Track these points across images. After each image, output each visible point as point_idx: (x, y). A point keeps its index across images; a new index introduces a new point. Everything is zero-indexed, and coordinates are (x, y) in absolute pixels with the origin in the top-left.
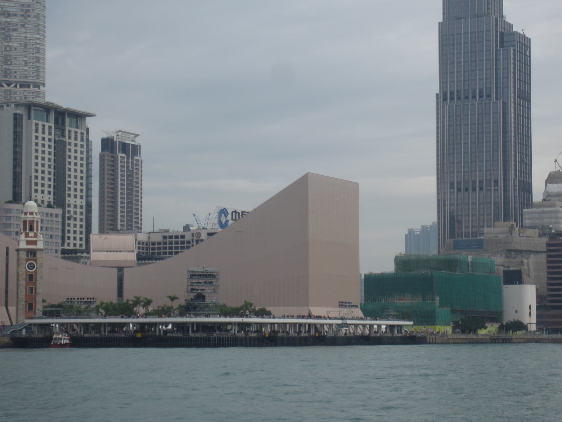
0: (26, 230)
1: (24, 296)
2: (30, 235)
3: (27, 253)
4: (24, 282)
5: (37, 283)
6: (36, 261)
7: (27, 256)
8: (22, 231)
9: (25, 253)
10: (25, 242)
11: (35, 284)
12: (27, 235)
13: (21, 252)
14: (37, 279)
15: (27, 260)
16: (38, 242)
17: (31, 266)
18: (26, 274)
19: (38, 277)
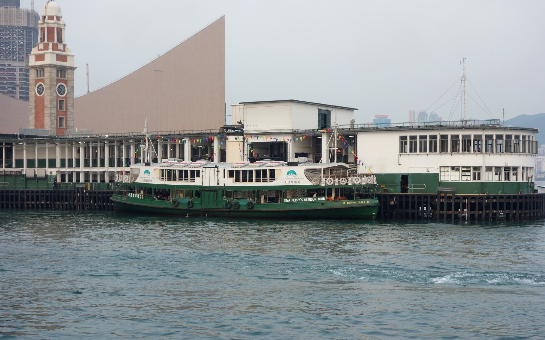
0: (54, 40)
1: (55, 130)
2: (59, 48)
3: (58, 71)
4: (55, 112)
5: (68, 113)
6: (66, 82)
7: (57, 76)
8: (46, 41)
9: (55, 71)
10: (55, 56)
11: (65, 113)
12: (55, 48)
13: (47, 70)
14: (69, 108)
15: (58, 82)
16: (68, 58)
17: (61, 90)
18: (57, 99)
19: (69, 104)
